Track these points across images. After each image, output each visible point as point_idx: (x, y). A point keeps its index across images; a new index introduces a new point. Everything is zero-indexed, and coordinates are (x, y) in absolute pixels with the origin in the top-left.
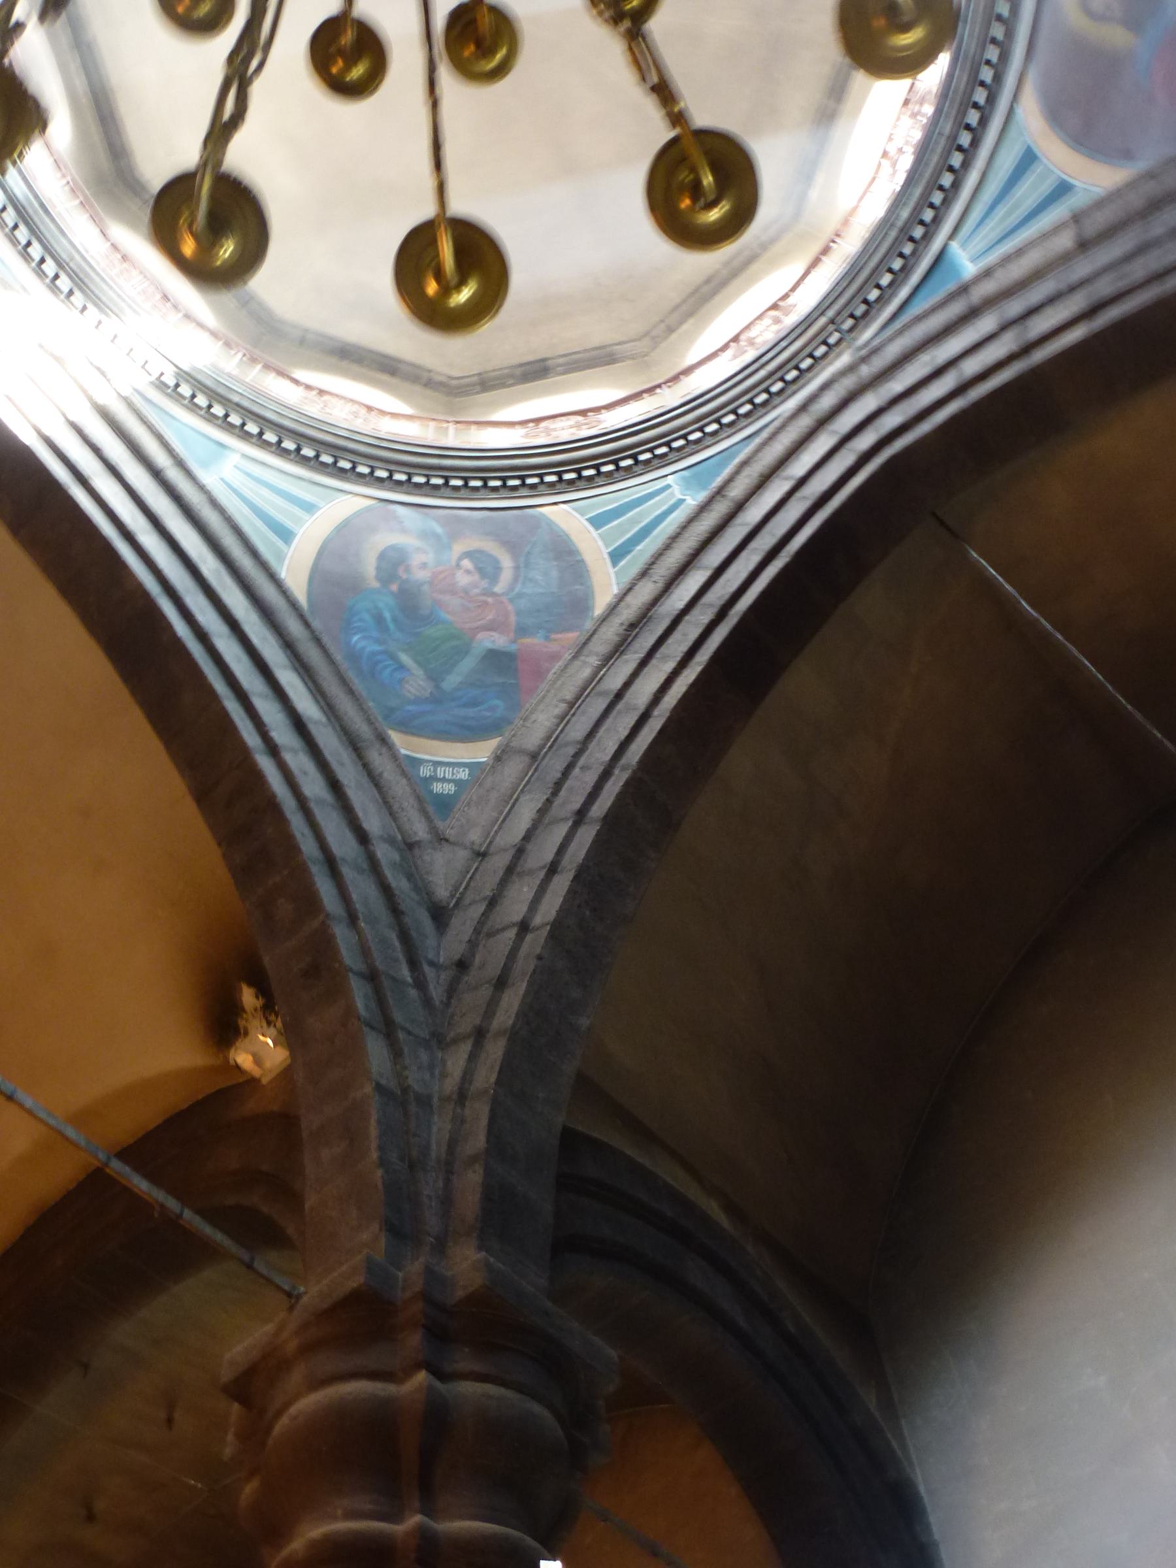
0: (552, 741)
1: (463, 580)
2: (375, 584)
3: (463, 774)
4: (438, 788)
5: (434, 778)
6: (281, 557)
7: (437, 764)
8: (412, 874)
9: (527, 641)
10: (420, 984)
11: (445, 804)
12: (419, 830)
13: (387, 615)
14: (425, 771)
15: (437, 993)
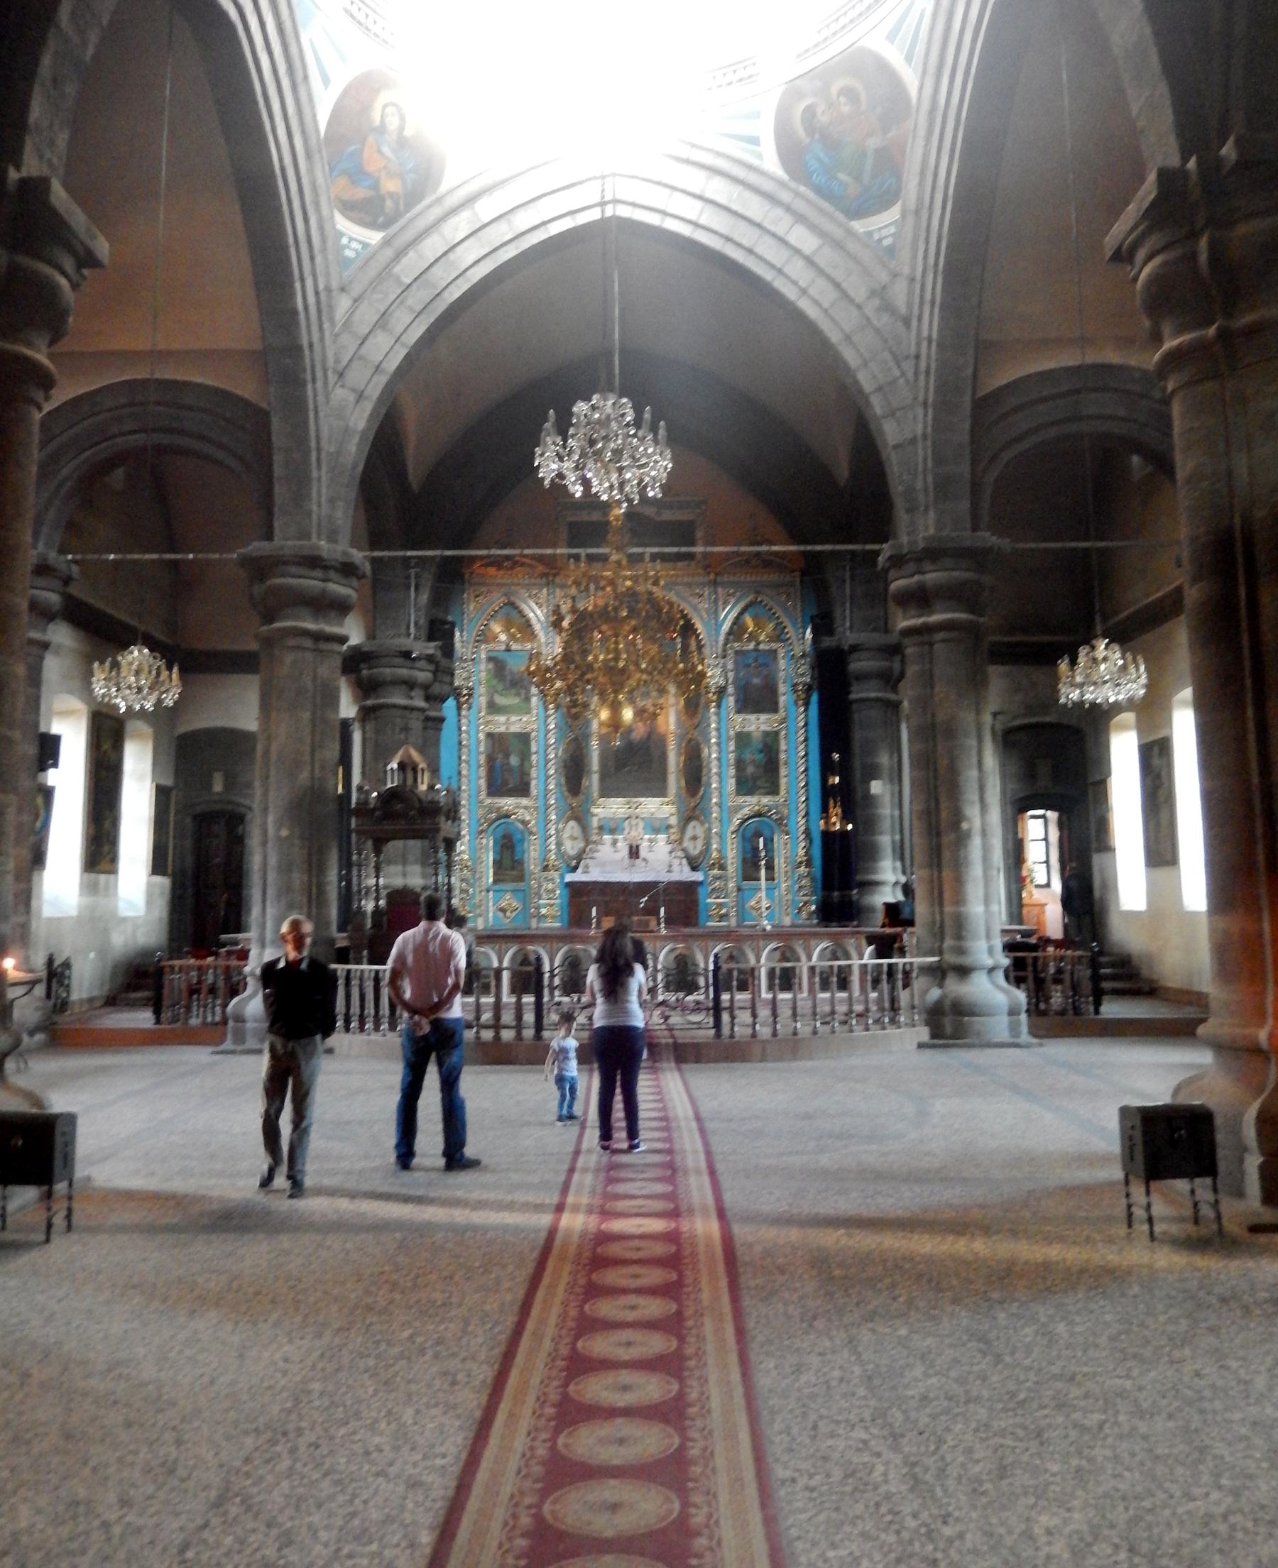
0: (920, 199)
1: (846, 109)
2: (808, 140)
3: (893, 230)
4: (886, 242)
5: (880, 240)
6: (760, 156)
7: (880, 229)
8: (888, 307)
9: (890, 135)
10: (903, 374)
11: (891, 251)
12: (884, 277)
13: (822, 155)
14: (876, 237)
15: (910, 375)
